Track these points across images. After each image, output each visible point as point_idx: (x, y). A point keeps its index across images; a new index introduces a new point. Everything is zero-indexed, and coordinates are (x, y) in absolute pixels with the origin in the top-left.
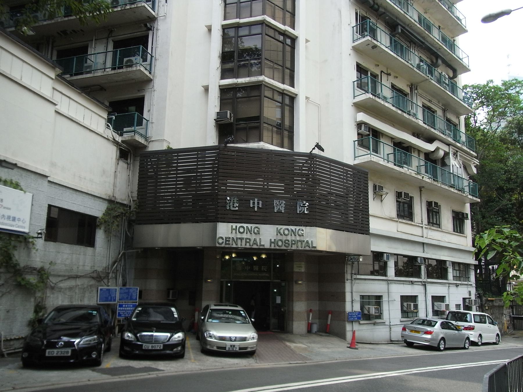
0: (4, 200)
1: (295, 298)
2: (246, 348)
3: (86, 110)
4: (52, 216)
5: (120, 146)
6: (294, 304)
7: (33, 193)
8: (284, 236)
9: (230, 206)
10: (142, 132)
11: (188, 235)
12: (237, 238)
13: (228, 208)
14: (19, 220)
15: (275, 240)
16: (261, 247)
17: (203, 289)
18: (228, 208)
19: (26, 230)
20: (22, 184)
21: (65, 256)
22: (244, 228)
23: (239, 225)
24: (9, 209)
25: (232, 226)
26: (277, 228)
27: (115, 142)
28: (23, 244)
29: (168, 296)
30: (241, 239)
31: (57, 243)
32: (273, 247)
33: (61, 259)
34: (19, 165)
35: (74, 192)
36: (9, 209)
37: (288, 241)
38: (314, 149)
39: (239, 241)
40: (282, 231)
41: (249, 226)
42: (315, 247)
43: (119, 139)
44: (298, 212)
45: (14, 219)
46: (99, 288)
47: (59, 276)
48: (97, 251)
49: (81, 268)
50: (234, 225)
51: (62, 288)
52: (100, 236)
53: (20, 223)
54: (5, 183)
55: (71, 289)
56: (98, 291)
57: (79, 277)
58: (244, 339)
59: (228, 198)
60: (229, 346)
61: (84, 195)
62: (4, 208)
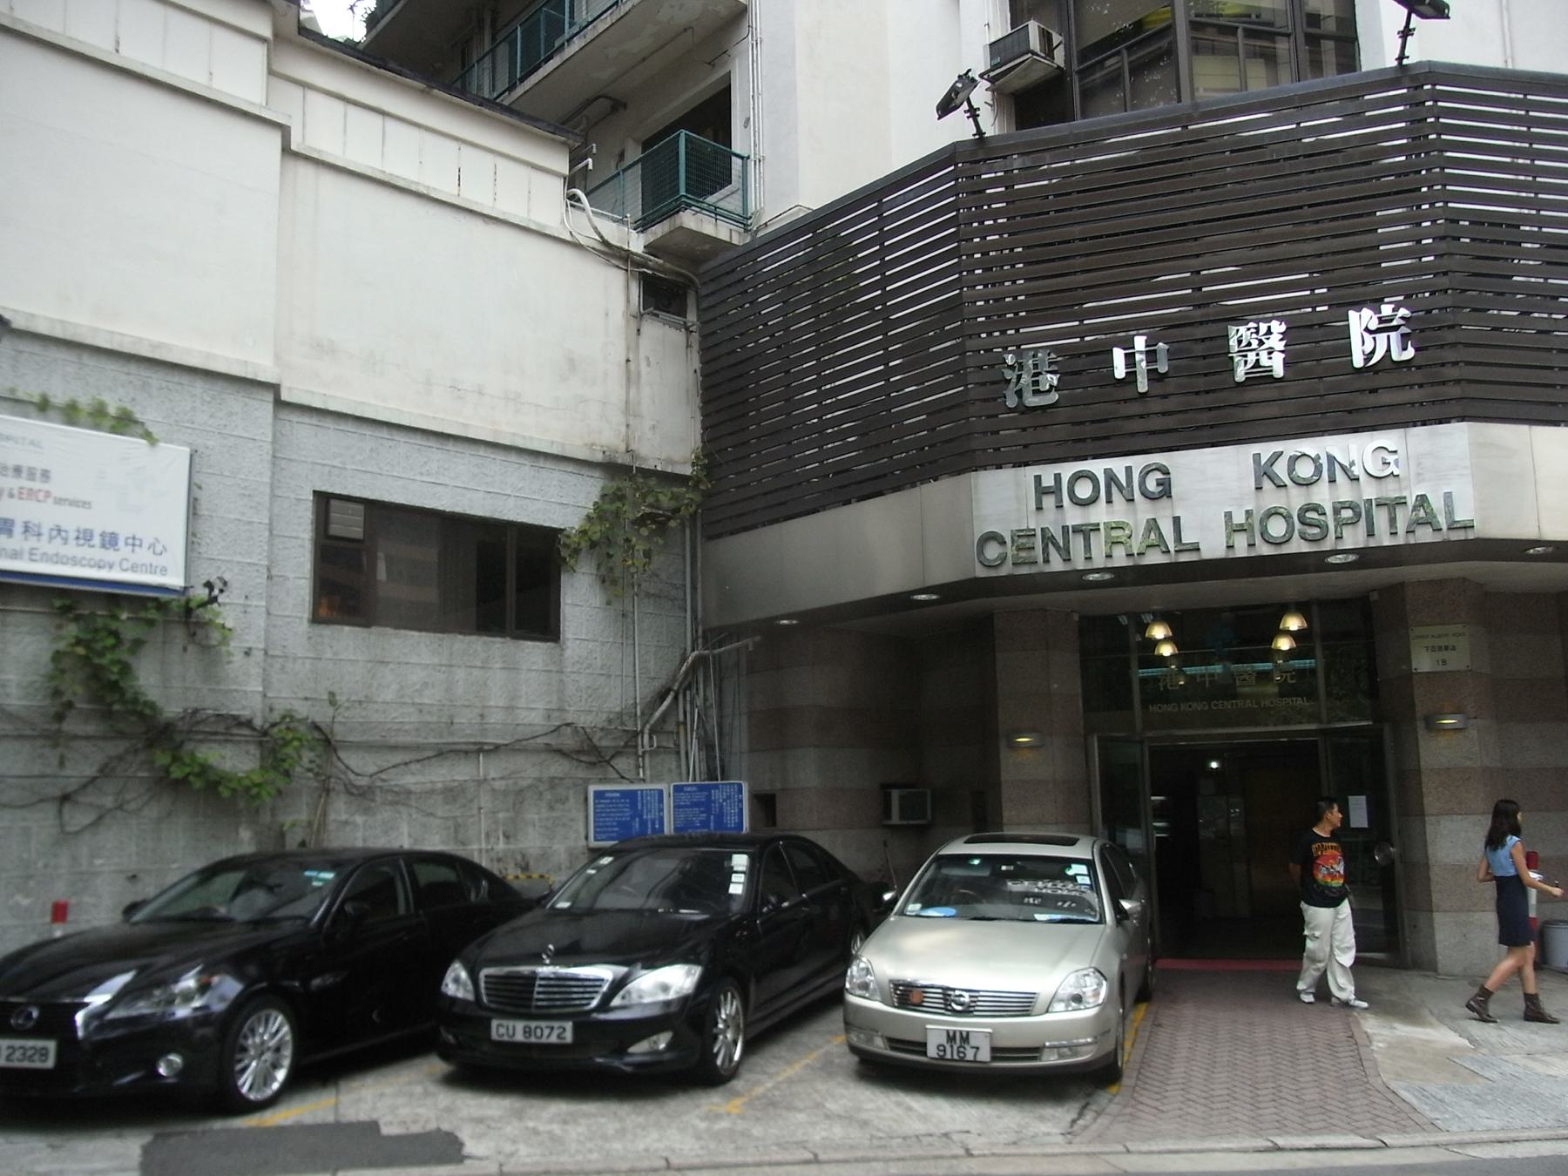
0: (53, 475)
1: (1430, 802)
2: (1034, 1051)
3: (466, 150)
4: (335, 529)
5: (639, 265)
6: (1429, 829)
7: (189, 444)
8: (1294, 490)
9: (1019, 393)
10: (732, 204)
11: (879, 546)
12: (1065, 529)
13: (1012, 402)
14: (134, 542)
15: (1249, 513)
16: (1184, 558)
17: (1004, 776)
18: (1012, 402)
19: (176, 580)
20: (147, 414)
21: (417, 676)
22: (1092, 478)
23: (1068, 470)
24: (86, 504)
25: (1038, 479)
26: (1257, 457)
27: (613, 254)
28: (179, 634)
29: (887, 813)
30: (1086, 531)
31: (374, 629)
32: (1241, 551)
33: (394, 687)
34: (18, 323)
35: (432, 442)
36: (86, 504)
37: (1316, 508)
38: (1406, 33)
39: (1077, 543)
40: (1281, 469)
41: (1118, 465)
42: (1468, 527)
43: (637, 244)
44: (1358, 362)
45: (110, 541)
46: (592, 789)
47: (395, 748)
48: (568, 653)
49: (495, 718)
50: (1047, 473)
51: (409, 792)
52: (580, 599)
53: (143, 555)
54: (16, 403)
55: (452, 793)
56: (586, 799)
57: (489, 751)
58: (1025, 1005)
59: (1010, 359)
60: (943, 1040)
61: (482, 451)
62: (59, 501)
